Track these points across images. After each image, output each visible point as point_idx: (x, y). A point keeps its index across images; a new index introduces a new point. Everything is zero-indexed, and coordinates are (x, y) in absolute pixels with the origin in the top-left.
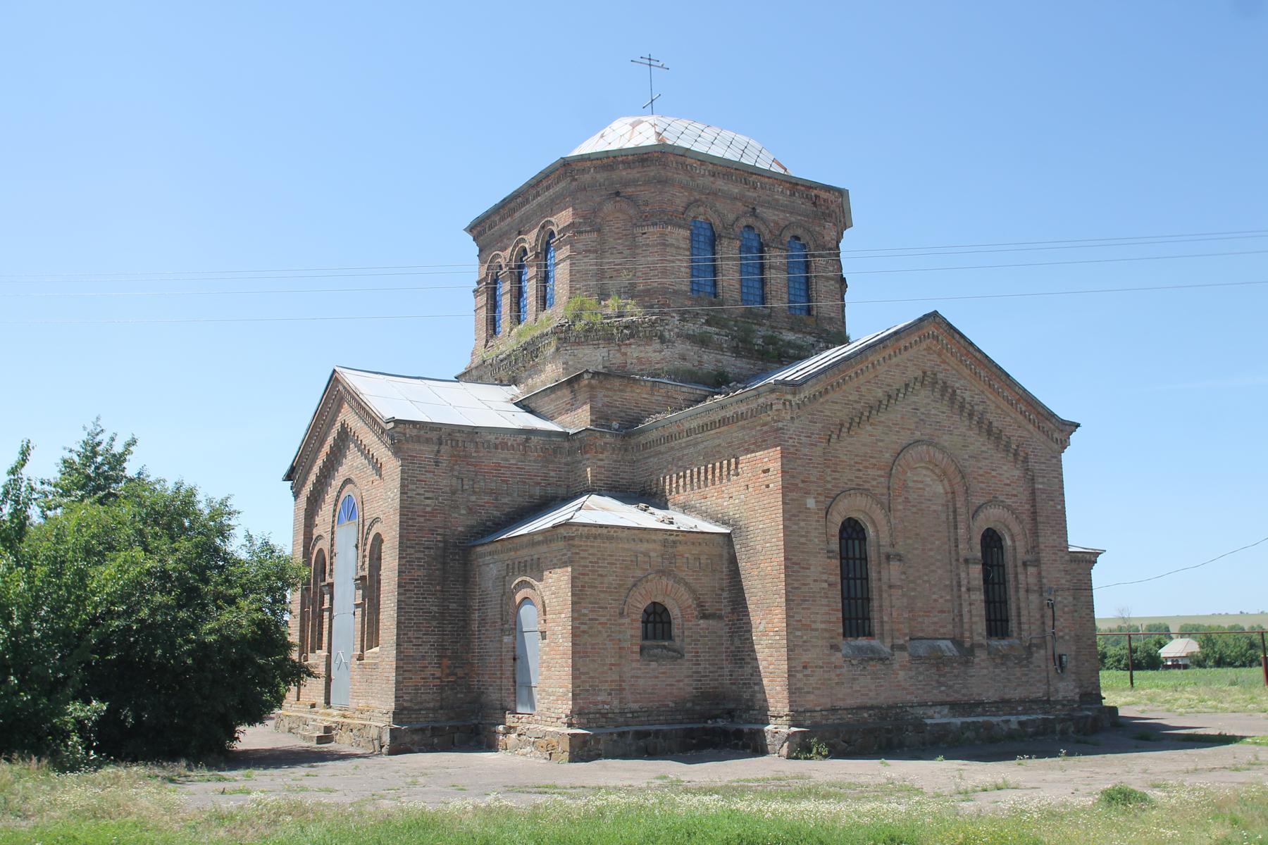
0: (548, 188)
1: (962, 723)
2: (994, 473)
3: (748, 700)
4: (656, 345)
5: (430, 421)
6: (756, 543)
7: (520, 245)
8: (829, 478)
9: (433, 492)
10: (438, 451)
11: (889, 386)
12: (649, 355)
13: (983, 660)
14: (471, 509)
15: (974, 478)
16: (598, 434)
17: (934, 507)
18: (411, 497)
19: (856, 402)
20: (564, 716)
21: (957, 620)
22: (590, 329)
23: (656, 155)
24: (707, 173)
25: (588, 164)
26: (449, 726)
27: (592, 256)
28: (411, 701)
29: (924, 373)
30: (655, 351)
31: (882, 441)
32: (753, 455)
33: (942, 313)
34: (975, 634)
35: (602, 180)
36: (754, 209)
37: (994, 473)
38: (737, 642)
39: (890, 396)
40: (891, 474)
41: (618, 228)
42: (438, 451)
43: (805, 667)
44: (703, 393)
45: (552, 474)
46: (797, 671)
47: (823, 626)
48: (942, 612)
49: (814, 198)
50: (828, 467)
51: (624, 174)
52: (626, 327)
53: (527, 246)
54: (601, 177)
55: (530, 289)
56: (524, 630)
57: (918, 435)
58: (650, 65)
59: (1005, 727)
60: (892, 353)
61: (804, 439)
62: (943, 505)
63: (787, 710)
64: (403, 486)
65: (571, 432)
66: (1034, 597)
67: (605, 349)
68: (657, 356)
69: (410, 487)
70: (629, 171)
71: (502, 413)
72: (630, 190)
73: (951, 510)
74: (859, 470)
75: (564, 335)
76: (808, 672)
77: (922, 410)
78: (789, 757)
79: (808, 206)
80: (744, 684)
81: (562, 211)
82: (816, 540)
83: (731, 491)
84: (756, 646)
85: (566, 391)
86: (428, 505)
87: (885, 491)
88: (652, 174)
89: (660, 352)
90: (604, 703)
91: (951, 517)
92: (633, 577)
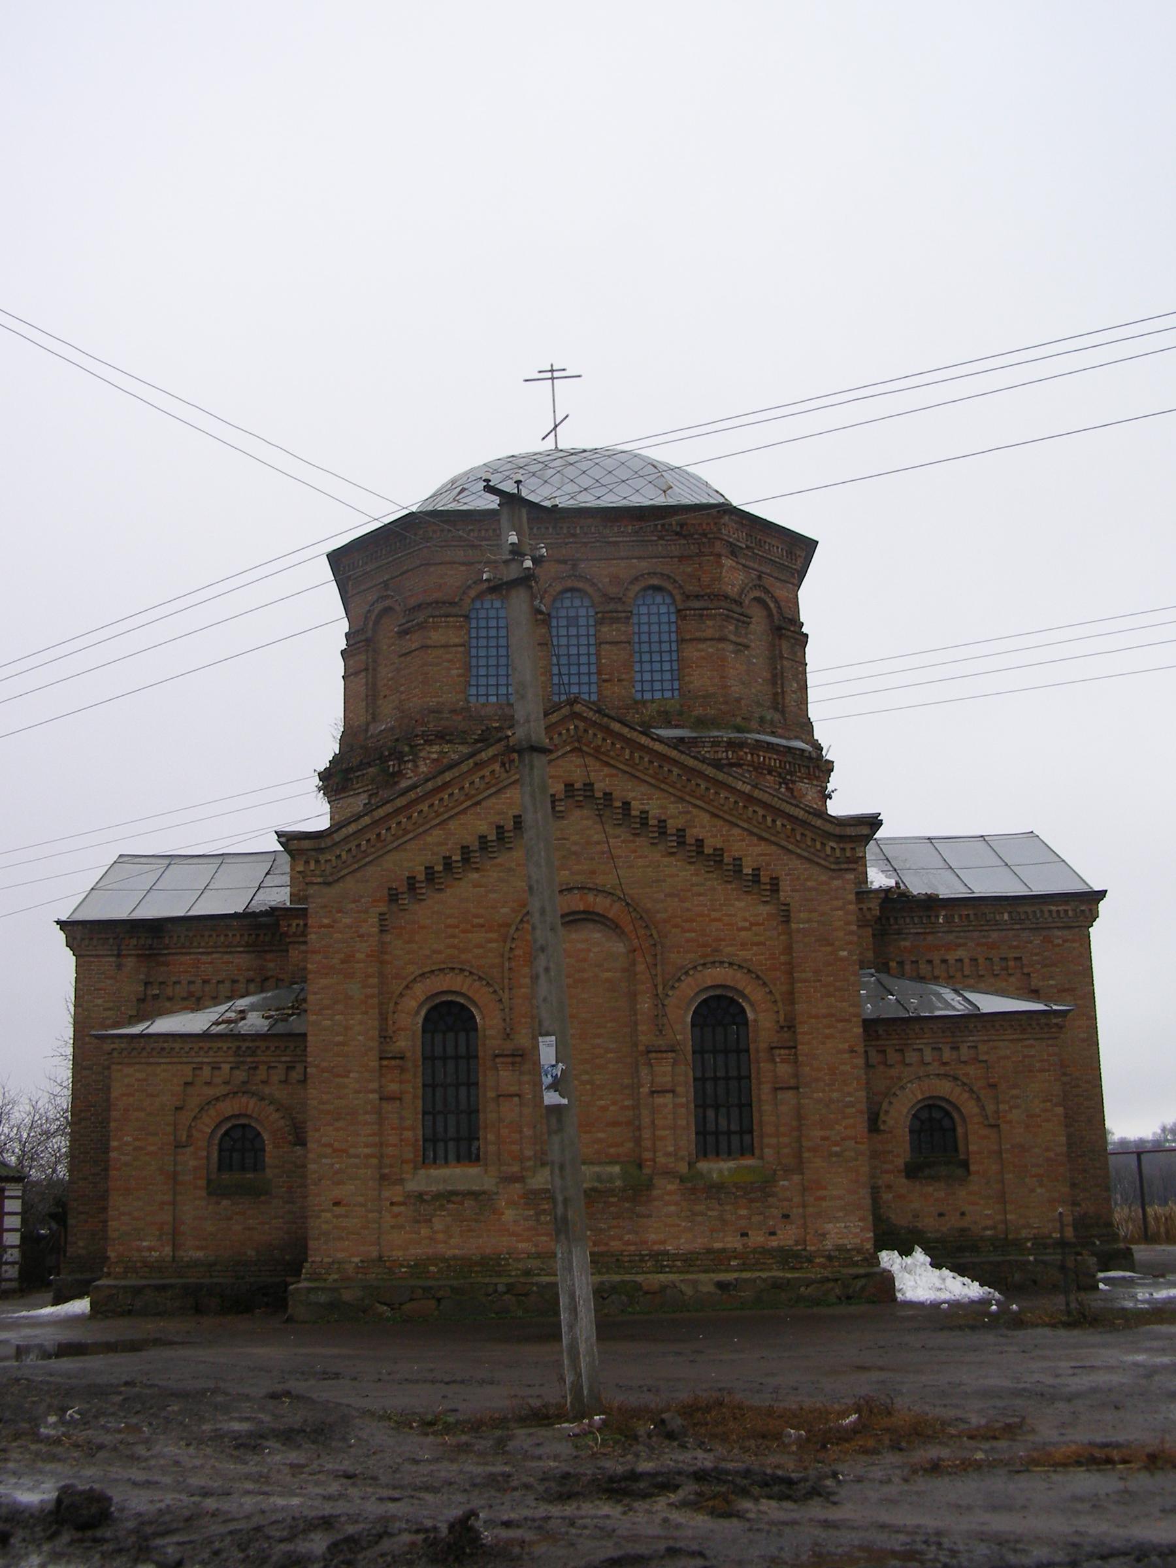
2: (714, 915)
13: (670, 1193)
15: (676, 926)
19: (440, 844)
29: (569, 786)
34: (659, 1154)
37: (714, 915)
43: (337, 1204)
45: (271, 965)
46: (323, 1211)
47: (367, 1151)
48: (615, 1124)
59: (689, 1291)
74: (453, 936)
76: (338, 1210)
77: (575, 838)
82: (360, 1038)
86: (107, 1018)
90: (150, 1249)
92: (199, 1095)
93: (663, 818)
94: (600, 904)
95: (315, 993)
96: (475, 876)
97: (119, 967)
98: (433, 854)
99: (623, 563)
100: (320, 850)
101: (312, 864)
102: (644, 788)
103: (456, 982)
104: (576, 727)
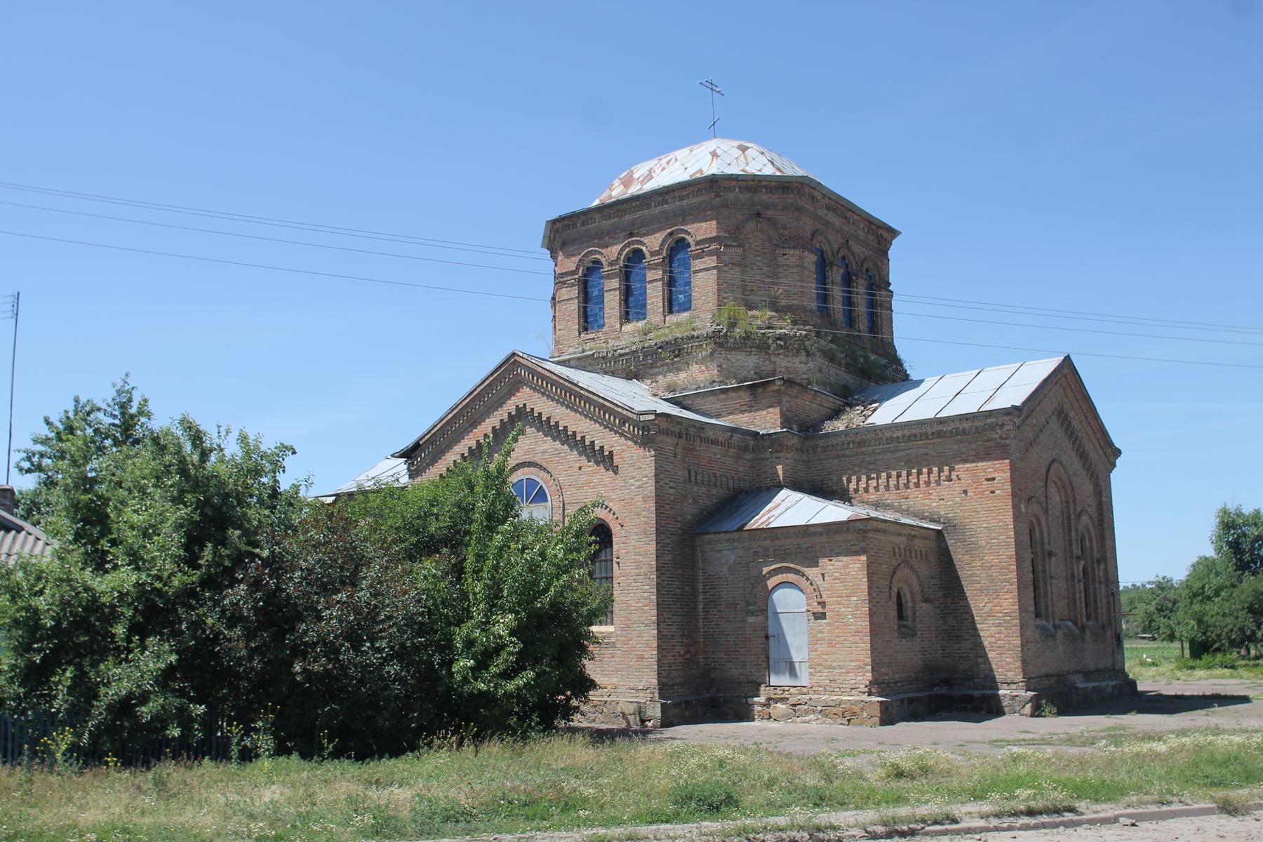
0: (681, 199)
1: (1093, 687)
3: (966, 671)
4: (803, 357)
6: (979, 539)
10: (677, 444)
16: (790, 436)
20: (863, 686)
21: (1071, 605)
22: (748, 336)
23: (796, 185)
25: (734, 183)
26: (696, 700)
27: (738, 269)
28: (666, 677)
30: (801, 363)
32: (974, 465)
35: (744, 200)
36: (847, 241)
38: (951, 622)
42: (677, 444)
44: (840, 403)
45: (741, 469)
51: (765, 197)
52: (779, 339)
54: (744, 197)
55: (655, 294)
56: (779, 611)
63: (1020, 677)
64: (656, 475)
66: (1103, 587)
67: (756, 357)
68: (803, 368)
70: (770, 195)
72: (770, 213)
75: (720, 341)
78: (1032, 715)
79: (875, 244)
80: (961, 657)
81: (700, 221)
84: (978, 626)
85: (745, 397)
86: (671, 494)
88: (790, 201)
89: (806, 364)
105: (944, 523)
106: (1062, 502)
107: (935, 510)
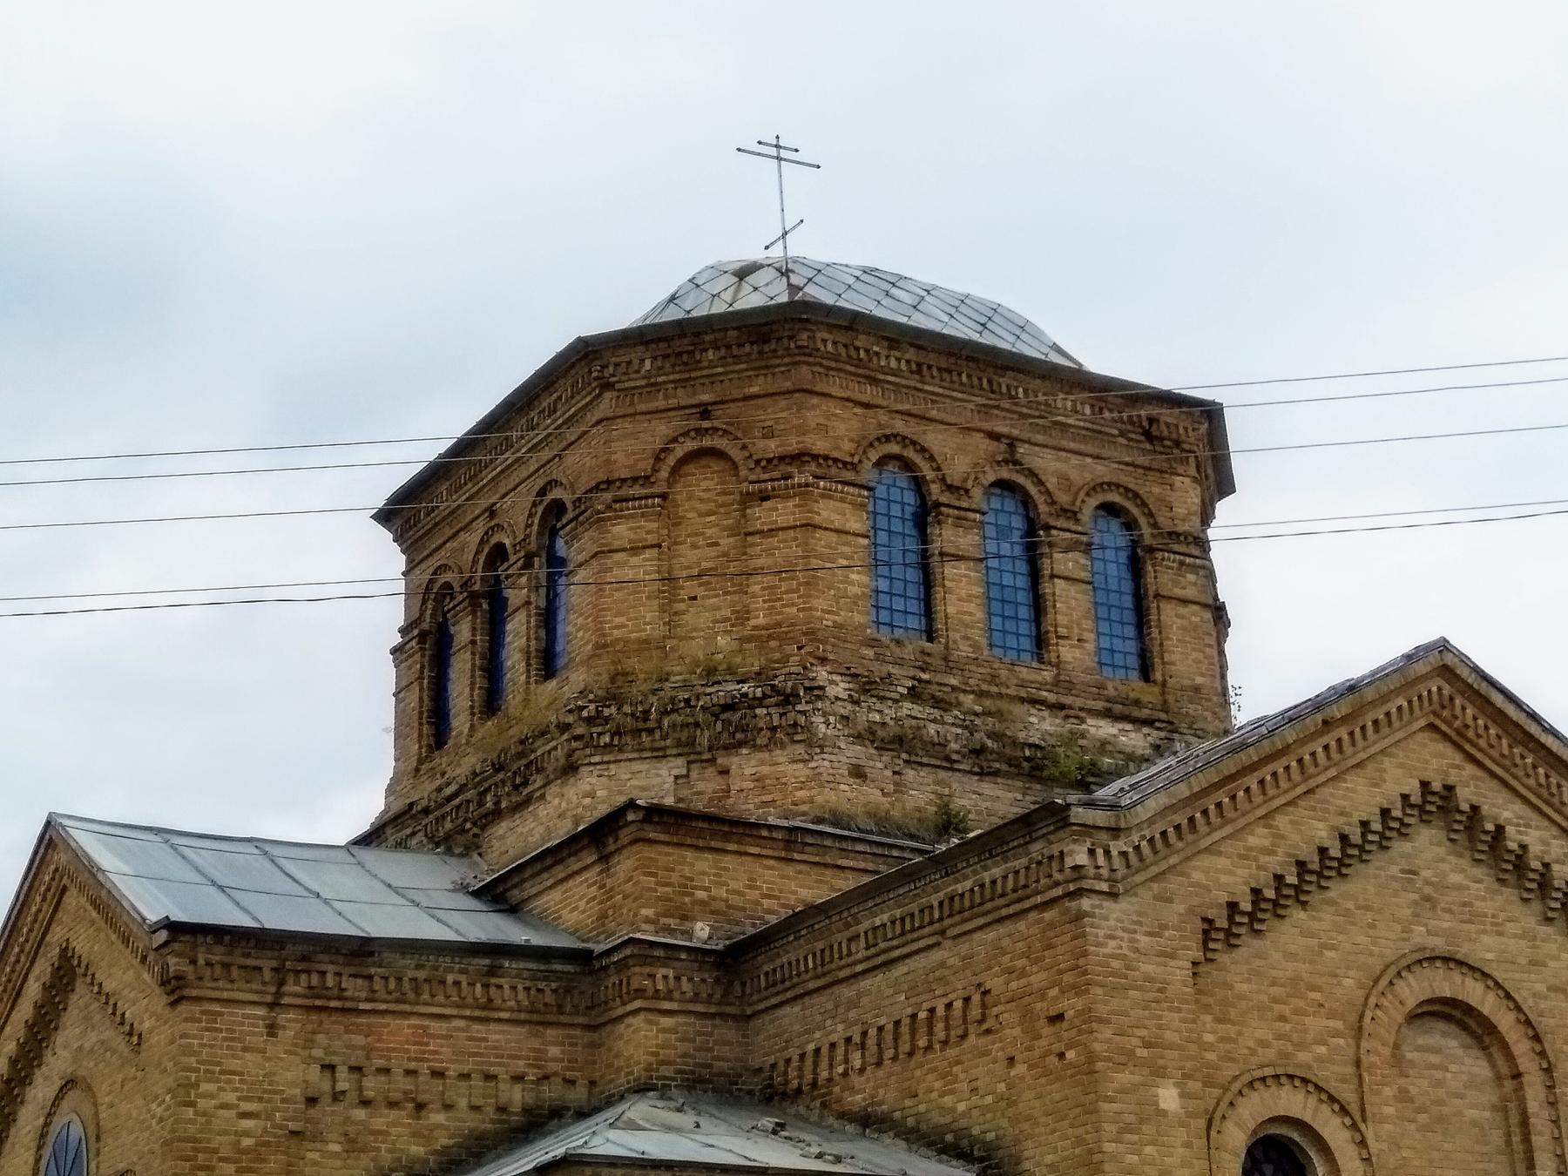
5: (247, 922)
7: (493, 541)
8: (1209, 1038)
9: (260, 1099)
11: (1342, 814)
12: (781, 768)
14: (353, 1141)
17: (1473, 1113)
18: (204, 1114)
24: (903, 365)
29: (1425, 785)
31: (1333, 948)
33: (1458, 642)
39: (1344, 838)
40: (1360, 1028)
41: (707, 490)
45: (554, 1051)
49: (1145, 424)
50: (1207, 1008)
53: (507, 542)
57: (1419, 935)
58: (779, 159)
60: (1345, 737)
61: (1144, 940)
62: (1494, 1108)
65: (599, 948)
69: (205, 1087)
71: (441, 914)
73: (1514, 1118)
74: (1282, 1018)
77: (1426, 873)
83: (975, 1072)
86: (246, 1133)
87: (1350, 1070)
91: (1516, 1139)
93: (1546, 860)
94: (1473, 992)
95: (1111, 1100)
96: (1299, 915)
97: (272, 1029)
98: (1259, 868)
99: (1075, 460)
100: (1115, 832)
101: (1100, 852)
102: (1518, 807)
103: (1292, 1102)
104: (1440, 689)
105: (981, 1160)
106: (1499, 1078)
107: (963, 1123)
